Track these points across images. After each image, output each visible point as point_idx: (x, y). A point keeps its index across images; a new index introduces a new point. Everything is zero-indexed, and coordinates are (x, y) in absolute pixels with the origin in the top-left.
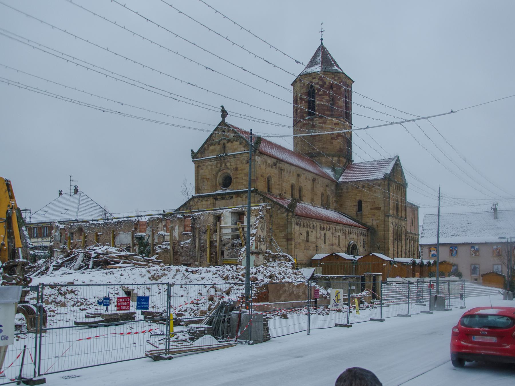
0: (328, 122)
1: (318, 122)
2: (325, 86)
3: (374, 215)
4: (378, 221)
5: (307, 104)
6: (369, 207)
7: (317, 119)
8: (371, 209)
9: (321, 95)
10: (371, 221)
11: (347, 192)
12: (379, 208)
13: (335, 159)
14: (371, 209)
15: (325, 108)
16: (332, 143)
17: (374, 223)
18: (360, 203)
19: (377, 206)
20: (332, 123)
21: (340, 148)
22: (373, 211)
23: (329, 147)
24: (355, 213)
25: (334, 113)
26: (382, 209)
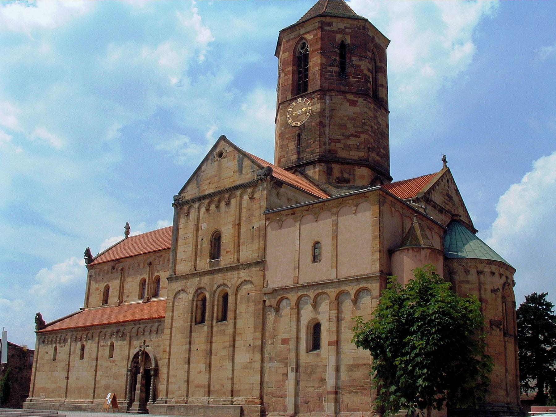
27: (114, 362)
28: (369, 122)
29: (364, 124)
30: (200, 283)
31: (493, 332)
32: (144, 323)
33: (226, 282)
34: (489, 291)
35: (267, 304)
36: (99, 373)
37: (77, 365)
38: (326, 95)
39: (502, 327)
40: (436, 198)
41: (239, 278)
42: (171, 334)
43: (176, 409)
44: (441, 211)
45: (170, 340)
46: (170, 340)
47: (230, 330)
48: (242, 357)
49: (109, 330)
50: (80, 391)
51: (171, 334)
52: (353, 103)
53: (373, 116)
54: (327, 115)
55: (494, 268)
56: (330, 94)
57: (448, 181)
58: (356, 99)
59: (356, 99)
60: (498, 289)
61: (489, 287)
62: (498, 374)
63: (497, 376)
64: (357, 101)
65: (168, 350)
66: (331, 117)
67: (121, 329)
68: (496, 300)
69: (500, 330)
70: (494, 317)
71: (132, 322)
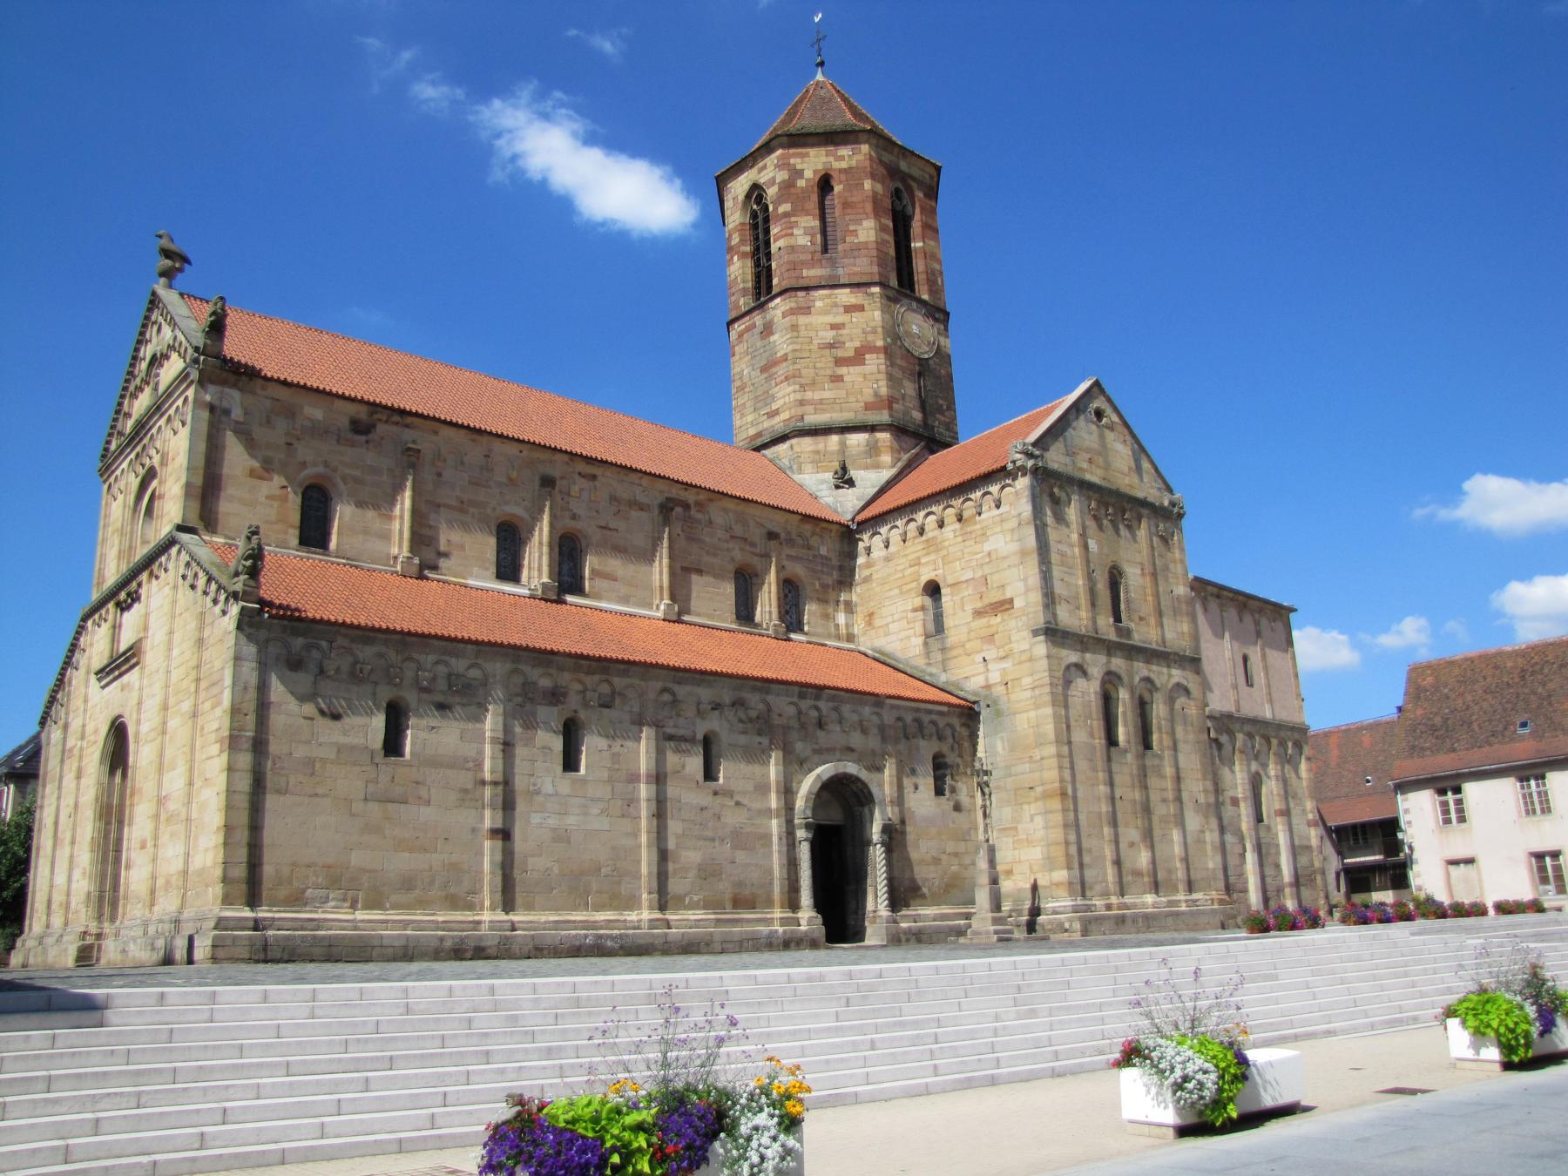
0: (818, 304)
1: (779, 313)
2: (801, 183)
3: (990, 639)
4: (1007, 664)
5: (749, 263)
6: (969, 608)
7: (778, 300)
8: (978, 613)
9: (786, 215)
10: (981, 667)
11: (887, 559)
12: (1004, 606)
13: (857, 440)
14: (978, 613)
15: (802, 257)
16: (837, 379)
17: (995, 677)
18: (933, 590)
19: (995, 596)
20: (836, 305)
21: (876, 394)
22: (983, 621)
23: (827, 395)
24: (920, 640)
25: (840, 271)
26: (1018, 603)
27: (729, 793)
30: (1109, 662)
32: (832, 699)
33: (1152, 676)
35: (1212, 734)
36: (674, 827)
37: (548, 788)
41: (1170, 676)
42: (1071, 755)
43: (1129, 922)
45: (1072, 768)
46: (1072, 768)
47: (1169, 771)
48: (1193, 821)
49: (705, 694)
50: (579, 885)
51: (1071, 755)
65: (1070, 792)
67: (754, 699)
71: (796, 689)
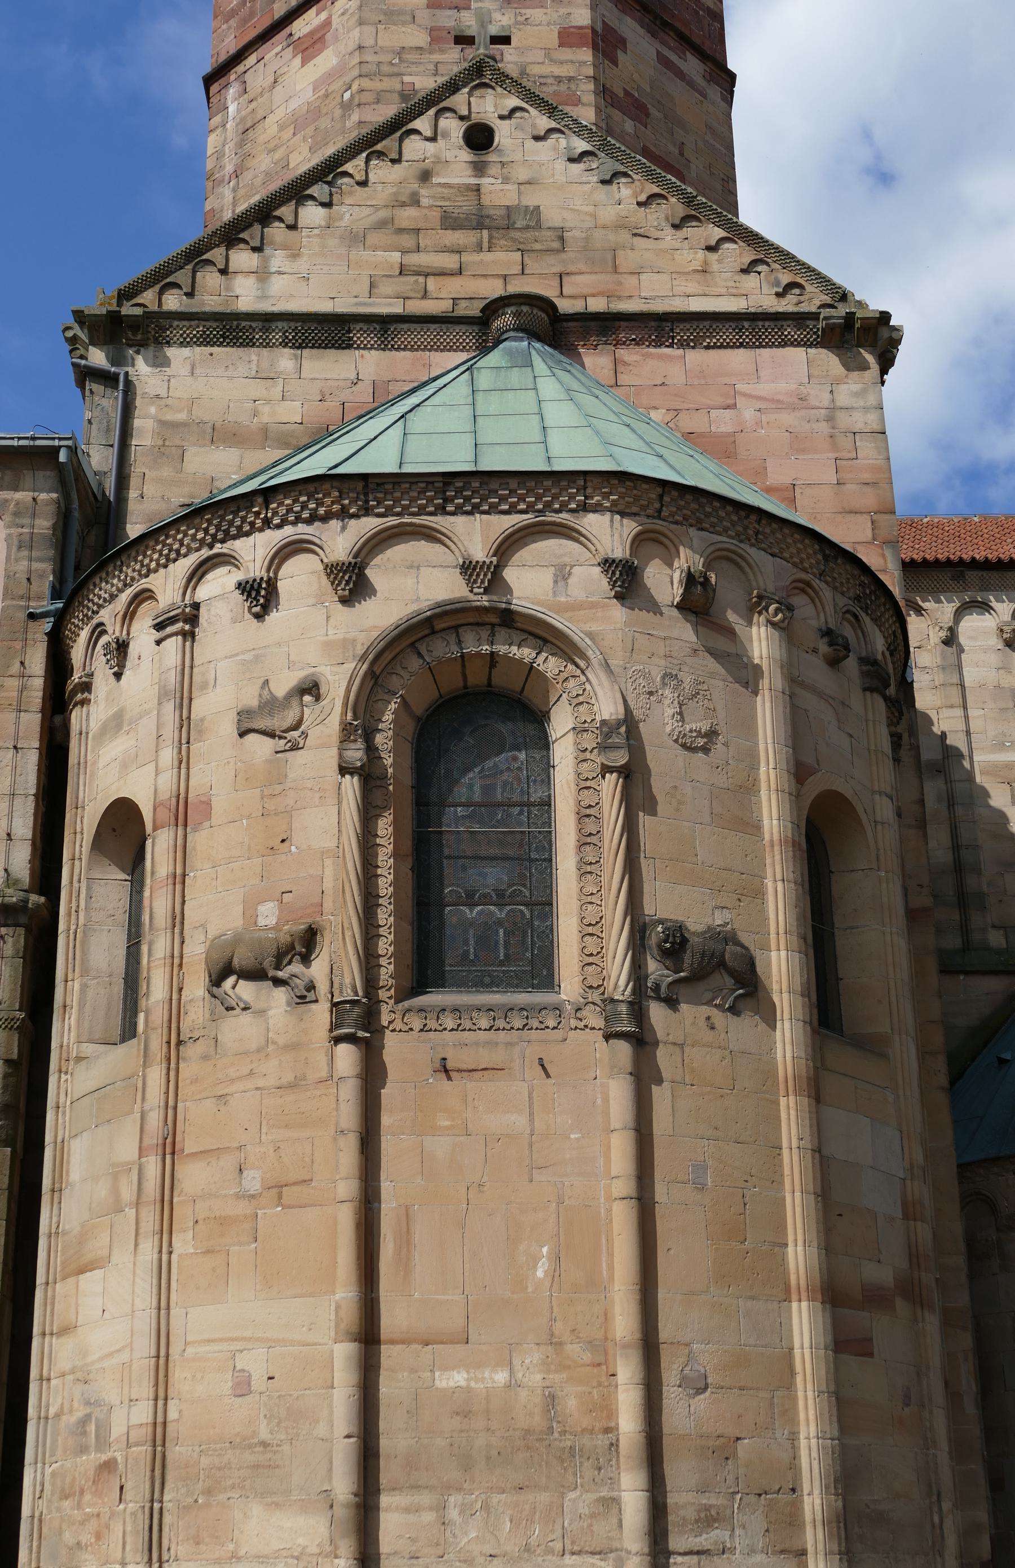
28: (387, 84)
29: (346, 107)
31: (239, 1029)
34: (228, 727)
38: (227, 85)
39: (318, 970)
40: (278, 285)
44: (326, 331)
52: (310, 47)
53: (421, 39)
54: (229, 168)
55: (253, 551)
56: (240, 68)
57: (479, 138)
58: (323, 16)
59: (323, 16)
60: (311, 689)
61: (218, 704)
62: (255, 1363)
63: (243, 1387)
64: (327, 23)
66: (236, 175)
68: (274, 778)
69: (306, 996)
70: (250, 914)
